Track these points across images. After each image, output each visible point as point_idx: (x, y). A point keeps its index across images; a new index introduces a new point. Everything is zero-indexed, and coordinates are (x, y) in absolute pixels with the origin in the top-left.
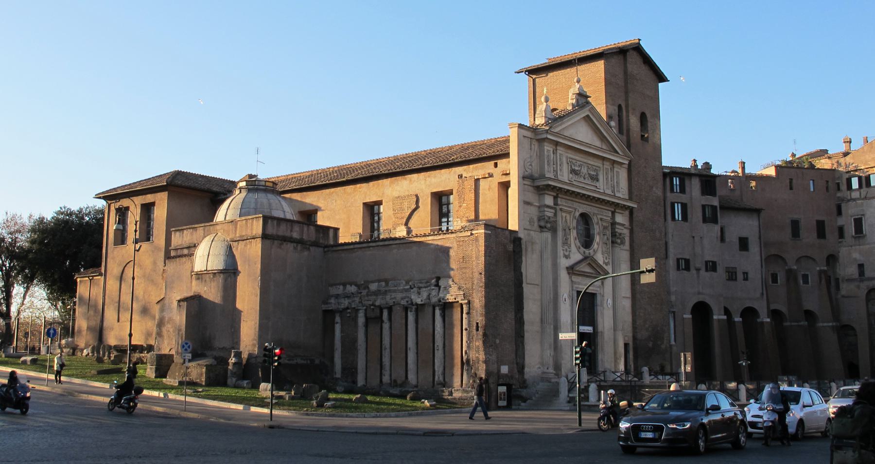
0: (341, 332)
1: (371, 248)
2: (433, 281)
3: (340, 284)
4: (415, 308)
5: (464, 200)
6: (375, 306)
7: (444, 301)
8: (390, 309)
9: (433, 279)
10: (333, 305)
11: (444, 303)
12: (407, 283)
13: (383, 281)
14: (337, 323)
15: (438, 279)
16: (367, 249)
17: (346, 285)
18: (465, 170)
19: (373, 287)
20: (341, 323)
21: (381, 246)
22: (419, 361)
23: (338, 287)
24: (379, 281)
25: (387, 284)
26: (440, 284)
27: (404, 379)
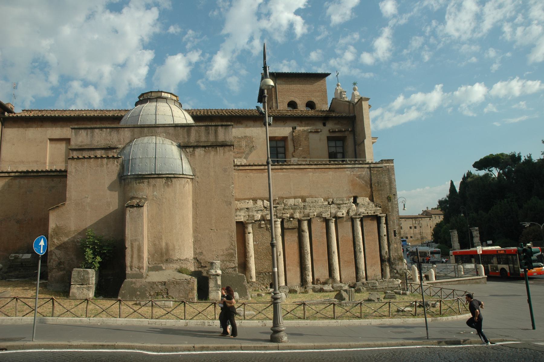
0: (253, 242)
1: (284, 170)
2: (352, 200)
3: (249, 199)
4: (335, 220)
5: (300, 145)
6: (293, 218)
7: (364, 215)
8: (310, 222)
9: (351, 197)
10: (242, 217)
11: (363, 216)
12: (326, 200)
13: (299, 198)
14: (249, 233)
15: (355, 198)
16: (280, 170)
17: (257, 201)
18: (298, 125)
19: (291, 202)
20: (253, 232)
21: (295, 169)
22: (341, 262)
24: (295, 198)
25: (304, 201)
26: (358, 202)
27: (327, 276)
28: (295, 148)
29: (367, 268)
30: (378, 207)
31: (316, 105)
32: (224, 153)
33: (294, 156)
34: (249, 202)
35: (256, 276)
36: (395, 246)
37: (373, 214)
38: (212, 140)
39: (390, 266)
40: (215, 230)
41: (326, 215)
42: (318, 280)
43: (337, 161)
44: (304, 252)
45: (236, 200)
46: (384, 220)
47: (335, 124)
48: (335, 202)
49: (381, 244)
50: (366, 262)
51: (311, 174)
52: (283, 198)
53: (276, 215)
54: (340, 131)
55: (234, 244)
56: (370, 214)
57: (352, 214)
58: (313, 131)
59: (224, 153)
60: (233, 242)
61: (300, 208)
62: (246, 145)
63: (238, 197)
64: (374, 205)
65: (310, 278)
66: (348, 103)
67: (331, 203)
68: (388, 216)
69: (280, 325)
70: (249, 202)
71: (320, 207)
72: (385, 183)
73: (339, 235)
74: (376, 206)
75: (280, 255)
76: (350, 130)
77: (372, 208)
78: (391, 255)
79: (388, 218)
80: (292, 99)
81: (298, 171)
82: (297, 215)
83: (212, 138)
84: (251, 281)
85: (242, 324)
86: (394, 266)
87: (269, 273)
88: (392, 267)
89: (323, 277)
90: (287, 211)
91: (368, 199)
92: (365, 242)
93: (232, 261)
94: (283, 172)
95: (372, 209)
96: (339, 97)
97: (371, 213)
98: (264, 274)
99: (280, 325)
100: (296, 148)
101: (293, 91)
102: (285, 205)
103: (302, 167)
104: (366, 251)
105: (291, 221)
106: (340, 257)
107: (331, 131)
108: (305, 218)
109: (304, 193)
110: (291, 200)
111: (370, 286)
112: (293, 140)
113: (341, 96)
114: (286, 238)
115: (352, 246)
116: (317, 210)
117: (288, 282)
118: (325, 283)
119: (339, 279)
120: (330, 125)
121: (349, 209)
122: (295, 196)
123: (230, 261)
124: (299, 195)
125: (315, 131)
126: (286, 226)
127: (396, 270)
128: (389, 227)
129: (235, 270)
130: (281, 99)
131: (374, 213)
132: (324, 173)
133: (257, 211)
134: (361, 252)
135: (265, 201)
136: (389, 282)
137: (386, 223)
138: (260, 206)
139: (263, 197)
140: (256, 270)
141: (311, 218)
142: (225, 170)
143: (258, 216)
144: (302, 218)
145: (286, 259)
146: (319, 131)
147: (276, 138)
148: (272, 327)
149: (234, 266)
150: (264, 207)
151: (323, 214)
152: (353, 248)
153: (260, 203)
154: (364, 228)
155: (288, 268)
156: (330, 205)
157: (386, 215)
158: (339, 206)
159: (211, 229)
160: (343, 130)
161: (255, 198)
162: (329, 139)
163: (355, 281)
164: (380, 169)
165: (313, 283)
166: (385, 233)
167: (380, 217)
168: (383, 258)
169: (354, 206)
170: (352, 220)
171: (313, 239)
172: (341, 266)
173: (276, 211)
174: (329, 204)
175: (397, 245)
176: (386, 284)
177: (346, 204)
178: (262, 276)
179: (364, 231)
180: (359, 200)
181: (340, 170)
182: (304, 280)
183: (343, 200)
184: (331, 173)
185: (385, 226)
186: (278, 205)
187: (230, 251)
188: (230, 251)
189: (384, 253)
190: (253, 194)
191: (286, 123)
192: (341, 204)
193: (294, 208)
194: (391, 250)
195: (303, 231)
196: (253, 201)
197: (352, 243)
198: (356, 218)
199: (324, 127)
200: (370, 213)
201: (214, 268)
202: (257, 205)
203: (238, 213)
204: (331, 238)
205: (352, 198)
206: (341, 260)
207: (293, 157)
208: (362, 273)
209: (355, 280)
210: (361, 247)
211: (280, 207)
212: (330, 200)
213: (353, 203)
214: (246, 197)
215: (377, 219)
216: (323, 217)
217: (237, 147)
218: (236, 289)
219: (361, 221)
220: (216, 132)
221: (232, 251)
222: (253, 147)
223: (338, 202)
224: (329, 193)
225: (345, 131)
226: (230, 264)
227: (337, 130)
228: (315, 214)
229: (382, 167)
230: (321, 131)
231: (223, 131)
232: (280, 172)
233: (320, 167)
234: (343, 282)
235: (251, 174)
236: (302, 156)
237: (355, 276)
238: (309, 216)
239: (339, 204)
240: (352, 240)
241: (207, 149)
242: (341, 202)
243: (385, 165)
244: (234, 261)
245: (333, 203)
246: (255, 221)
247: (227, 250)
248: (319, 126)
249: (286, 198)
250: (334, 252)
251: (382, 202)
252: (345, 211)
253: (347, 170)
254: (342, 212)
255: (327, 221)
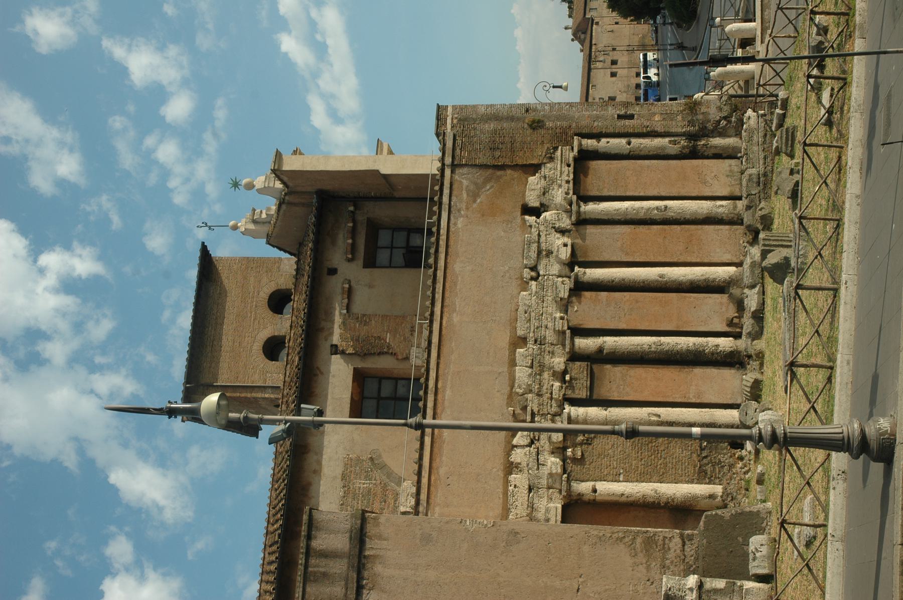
1: (440, 385)
2: (531, 219)
3: (507, 482)
4: (579, 267)
6: (565, 372)
7: (571, 192)
8: (578, 331)
9: (524, 221)
10: (551, 505)
11: (574, 194)
12: (524, 285)
13: (515, 355)
14: (595, 491)
15: (528, 210)
16: (440, 397)
17: (512, 463)
18: (326, 340)
19: (522, 374)
20: (592, 480)
23: (511, 488)
24: (513, 363)
25: (524, 340)
26: (537, 204)
27: (722, 298)
28: (386, 353)
29: (710, 194)
30: (554, 153)
31: (280, 288)
32: (380, 537)
33: (405, 356)
34: (513, 483)
35: (709, 483)
36: (657, 118)
37: (571, 169)
38: (345, 568)
39: (708, 136)
40: (581, 580)
41: (564, 288)
42: (730, 323)
43: (428, 248)
44: (655, 352)
45: (507, 517)
46: (590, 141)
47: (334, 243)
48: (532, 263)
49: (651, 153)
50: (693, 195)
51: (456, 319)
52: (511, 396)
53: (555, 415)
54: (353, 233)
55: (621, 535)
56: (572, 176)
57: (566, 223)
58: (346, 301)
59: (380, 537)
60: (616, 535)
61: (541, 352)
62: (366, 478)
63: (498, 511)
64: (548, 165)
65: (725, 344)
66: (284, 207)
67: (533, 274)
68: (580, 131)
69: (845, 434)
70: (513, 483)
71: (543, 302)
72: (495, 131)
73: (619, 259)
74: (551, 159)
75: (659, 416)
76: (351, 208)
77: (555, 169)
78: (680, 130)
79: (584, 132)
80: (258, 346)
81: (445, 350)
82: (559, 362)
83: (339, 567)
84: (722, 497)
85: (839, 534)
86: (710, 126)
87: (702, 449)
88: (712, 131)
89: (724, 309)
90: (545, 387)
91: (531, 179)
92: (642, 194)
93: (664, 544)
94: (444, 387)
95: (559, 169)
96: (266, 229)
97: (568, 173)
98: (705, 461)
99: (845, 434)
100: (385, 350)
101: (237, 344)
102: (531, 391)
103: (435, 340)
104: (663, 194)
105: (571, 378)
106: (675, 260)
107: (350, 256)
108: (568, 342)
109: (504, 340)
110: (517, 375)
111: (757, 191)
112: (364, 355)
113: (264, 223)
114: (615, 396)
115: (649, 229)
116: (550, 310)
117: (730, 402)
118: (740, 306)
119: (732, 269)
120: (337, 257)
121: (554, 228)
122: (509, 363)
123: (664, 548)
124: (507, 353)
125: (346, 296)
126: (583, 394)
127: (719, 122)
128: (608, 131)
129: (691, 538)
130: (256, 376)
131: (569, 166)
132: (455, 284)
133: (538, 464)
134: (666, 207)
135: (515, 442)
136: (750, 139)
137: (598, 136)
138: (525, 454)
139: (503, 445)
140: (692, 482)
141: (569, 328)
142: (426, 539)
143: (553, 463)
144: (567, 350)
145: (671, 400)
146: (347, 286)
147: (356, 398)
148: (851, 454)
149: (677, 540)
150: (530, 445)
151: (561, 295)
152: (655, 227)
153: (518, 456)
154: (606, 193)
155: (694, 397)
156: (539, 275)
157: (576, 135)
158: (544, 253)
159: (578, 591)
160: (351, 225)
161: (505, 468)
162: (370, 263)
163: (740, 229)
164: (459, 142)
165: (737, 336)
166: (623, 141)
167: (581, 151)
168: (687, 151)
169: (546, 215)
170: (582, 222)
171: (622, 326)
172: (698, 260)
173: (542, 415)
174: (535, 279)
175: (655, 114)
176: (755, 148)
177: (539, 235)
178: (709, 468)
179: (612, 194)
180: (534, 203)
181: (451, 242)
182: (729, 360)
183: (530, 243)
184: (458, 266)
185: (604, 140)
186: (529, 408)
187: (638, 546)
188: (638, 546)
189: (674, 149)
190: (495, 470)
191: (318, 368)
192: (539, 247)
193: (538, 367)
194: (667, 130)
195: (600, 350)
196: (511, 474)
197: (642, 229)
198: (579, 213)
199: (339, 272)
200: (568, 175)
201: (680, 593)
202: (524, 464)
203: (540, 515)
204: (623, 280)
205: (527, 217)
206: (682, 259)
207: (407, 358)
208: (722, 207)
209: (739, 227)
210: (653, 206)
211: (533, 403)
212: (527, 274)
213: (538, 217)
214: (501, 490)
215: (584, 158)
216: (569, 296)
217: (368, 503)
218: (740, 539)
219: (587, 199)
220: (325, 555)
221: (639, 540)
222: (372, 459)
223: (533, 255)
224: (508, 275)
225: (354, 221)
226: (672, 550)
227: (350, 241)
228: (558, 315)
229: (455, 136)
230: (349, 282)
231: (324, 536)
232: (444, 396)
233: (441, 291)
234: (742, 258)
235: (442, 471)
236: (408, 335)
237: (727, 227)
238: (564, 333)
239: (539, 252)
240: (633, 226)
241: (367, 584)
242: (534, 247)
243: (449, 126)
244: (665, 538)
245: (534, 268)
246: (564, 473)
247: (636, 555)
248: (335, 285)
249: (512, 387)
250: (661, 276)
251: (543, 143)
252: (558, 238)
253: (455, 224)
254: (561, 246)
255: (580, 288)
